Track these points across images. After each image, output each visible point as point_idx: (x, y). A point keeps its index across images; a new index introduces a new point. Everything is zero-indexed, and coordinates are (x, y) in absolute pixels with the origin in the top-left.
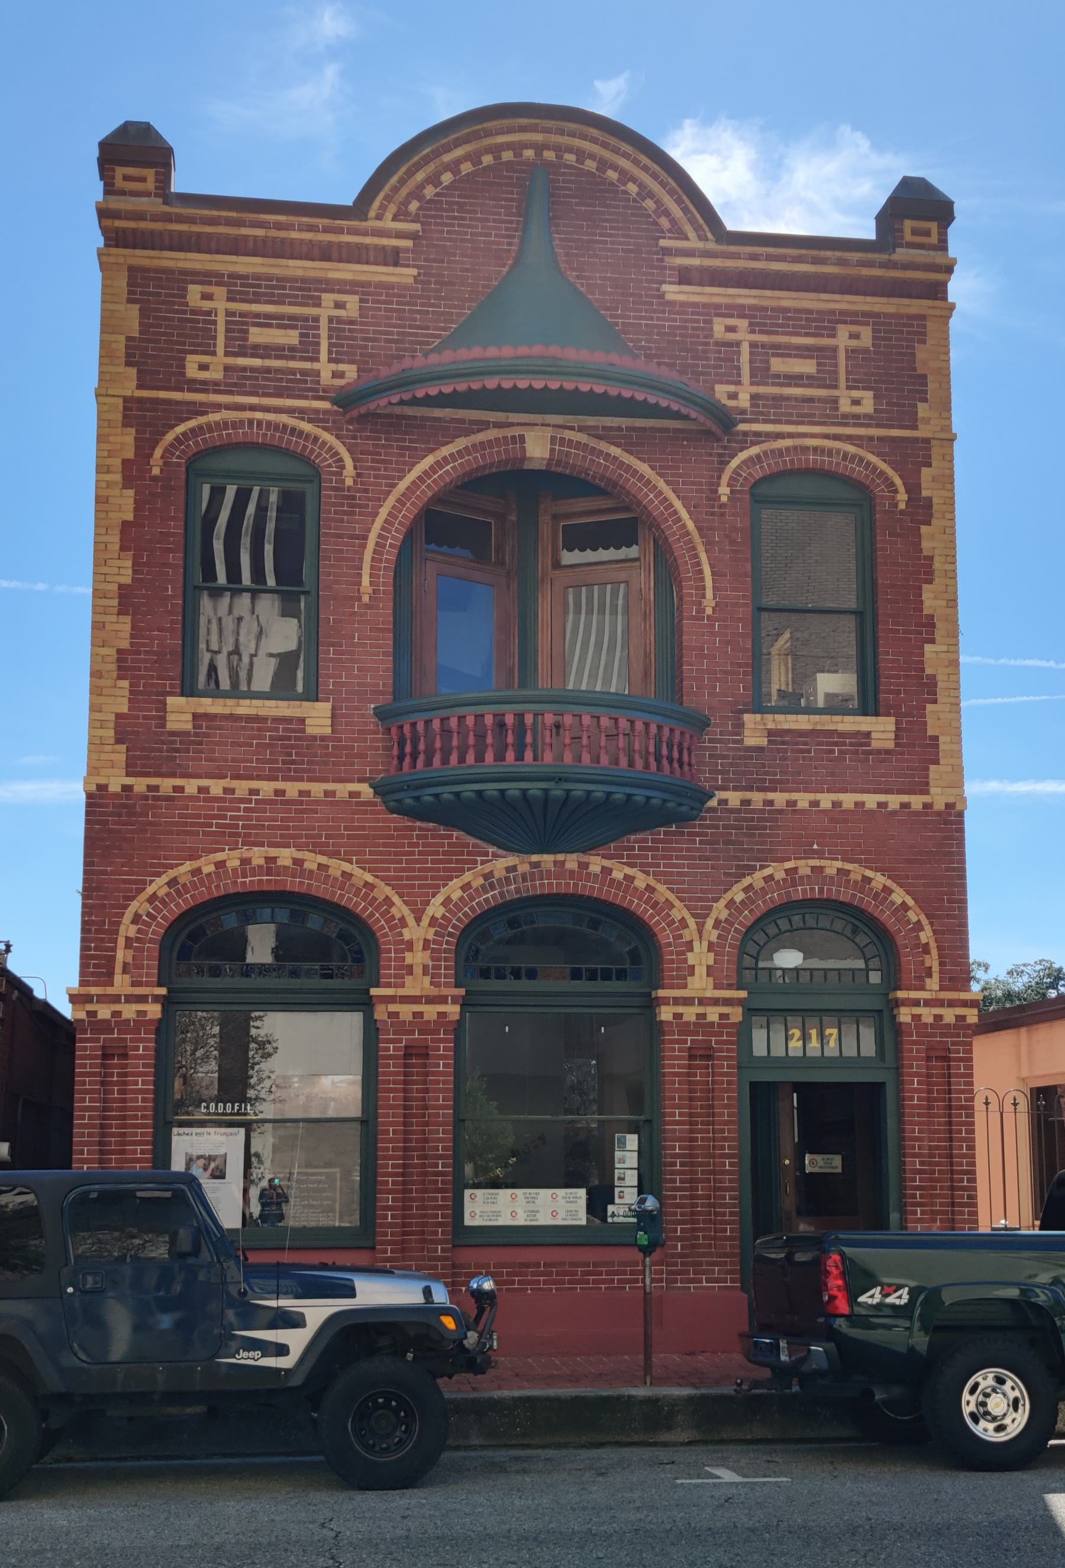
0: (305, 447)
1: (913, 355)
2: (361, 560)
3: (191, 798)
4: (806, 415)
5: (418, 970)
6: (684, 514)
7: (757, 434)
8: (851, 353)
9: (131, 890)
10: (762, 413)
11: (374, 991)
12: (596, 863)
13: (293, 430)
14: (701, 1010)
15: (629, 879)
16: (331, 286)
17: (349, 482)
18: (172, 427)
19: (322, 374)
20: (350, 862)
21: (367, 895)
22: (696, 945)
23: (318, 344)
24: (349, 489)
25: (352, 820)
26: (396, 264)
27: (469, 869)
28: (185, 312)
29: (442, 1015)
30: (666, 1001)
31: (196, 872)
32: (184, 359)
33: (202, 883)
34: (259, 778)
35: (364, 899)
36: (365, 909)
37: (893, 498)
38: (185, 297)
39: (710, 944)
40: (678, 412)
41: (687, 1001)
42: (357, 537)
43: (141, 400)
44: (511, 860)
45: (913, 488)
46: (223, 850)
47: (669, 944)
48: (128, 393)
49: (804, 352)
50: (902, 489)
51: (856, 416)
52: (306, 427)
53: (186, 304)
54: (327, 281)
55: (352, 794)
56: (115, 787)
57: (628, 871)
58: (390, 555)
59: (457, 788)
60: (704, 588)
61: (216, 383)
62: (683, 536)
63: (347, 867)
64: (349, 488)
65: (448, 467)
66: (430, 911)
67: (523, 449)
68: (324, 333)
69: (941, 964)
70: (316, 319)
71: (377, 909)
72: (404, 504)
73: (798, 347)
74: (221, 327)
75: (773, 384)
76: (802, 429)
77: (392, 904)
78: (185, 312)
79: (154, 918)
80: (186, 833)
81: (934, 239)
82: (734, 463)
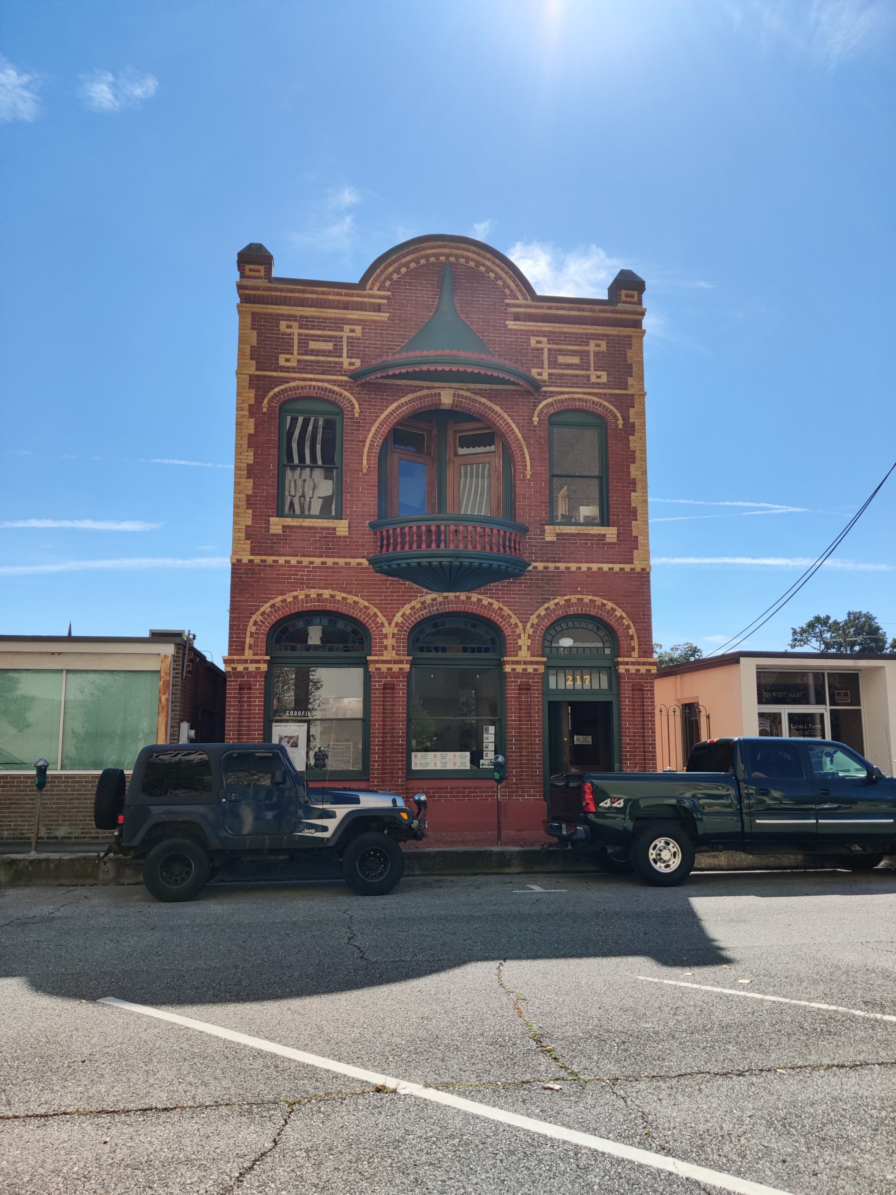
3: (282, 566)
5: (390, 648)
7: (551, 392)
8: (596, 354)
11: (369, 658)
12: (475, 597)
13: (330, 390)
17: (357, 415)
26: (379, 311)
30: (508, 662)
34: (314, 556)
41: (518, 663)
43: (257, 376)
44: (434, 595)
45: (626, 418)
48: (252, 373)
50: (620, 418)
51: (599, 384)
52: (336, 389)
54: (346, 319)
55: (358, 564)
58: (377, 450)
63: (356, 599)
67: (440, 400)
68: (345, 344)
73: (571, 351)
79: (263, 623)
82: (541, 406)
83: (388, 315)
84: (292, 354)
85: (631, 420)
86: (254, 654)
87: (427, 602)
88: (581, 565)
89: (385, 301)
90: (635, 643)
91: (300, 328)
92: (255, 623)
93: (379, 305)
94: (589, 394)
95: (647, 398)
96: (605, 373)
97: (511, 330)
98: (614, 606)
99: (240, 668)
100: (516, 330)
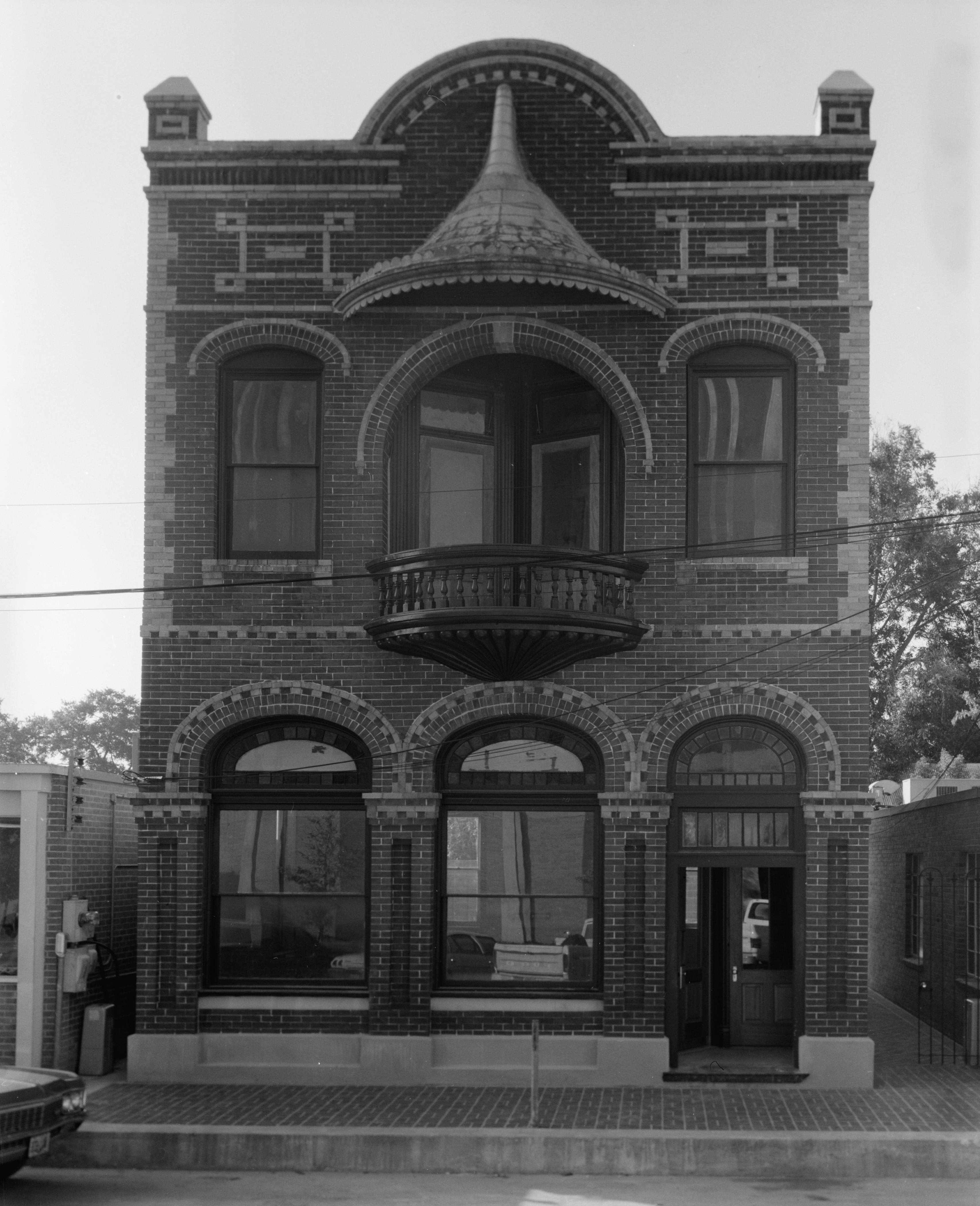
0: (311, 346)
1: (835, 231)
2: (356, 439)
3: (223, 641)
4: (737, 292)
5: (402, 778)
6: (627, 385)
7: (694, 311)
8: (780, 233)
9: (177, 716)
10: (698, 293)
11: (365, 796)
12: (549, 689)
13: (302, 331)
14: (635, 809)
15: (577, 700)
16: (330, 205)
17: (346, 373)
18: (204, 335)
19: (325, 282)
20: (348, 690)
21: (361, 717)
22: (633, 756)
23: (321, 257)
24: (347, 379)
25: (350, 657)
26: (386, 182)
27: (444, 695)
28: (213, 237)
29: (421, 814)
30: (605, 802)
31: (227, 700)
32: (213, 277)
33: (232, 709)
34: (276, 623)
35: (359, 720)
36: (360, 728)
37: (814, 362)
38: (213, 223)
39: (644, 753)
40: (609, 295)
41: (623, 802)
42: (353, 420)
43: (180, 314)
44: (479, 687)
45: (832, 353)
46: (248, 682)
47: (610, 755)
48: (169, 308)
49: (737, 235)
50: (821, 354)
51: (783, 291)
52: (311, 328)
53: (214, 230)
54: (330, 201)
55: (349, 635)
56: (164, 633)
57: (575, 693)
58: (380, 435)
59: (509, 626)
60: (644, 450)
61: (240, 295)
62: (627, 405)
63: (344, 694)
64: (347, 378)
65: (428, 356)
66: (413, 729)
67: (491, 337)
68: (326, 246)
69: (843, 768)
70: (320, 235)
71: (369, 728)
72: (391, 390)
73: (733, 231)
74: (243, 247)
75: (710, 266)
76: (733, 305)
77: (382, 724)
78: (213, 237)
79: (195, 737)
80: (219, 669)
81: (858, 123)
82: (673, 338)
83: (399, 187)
84: (237, 270)
85: (842, 356)
86: (182, 790)
87: (467, 699)
88: (740, 627)
89: (396, 163)
90: (836, 765)
91: (249, 223)
92: (182, 739)
93: (386, 169)
94: (765, 310)
95: (874, 315)
96: (796, 269)
97: (621, 199)
98: (800, 700)
99: (158, 812)
100: (630, 199)
